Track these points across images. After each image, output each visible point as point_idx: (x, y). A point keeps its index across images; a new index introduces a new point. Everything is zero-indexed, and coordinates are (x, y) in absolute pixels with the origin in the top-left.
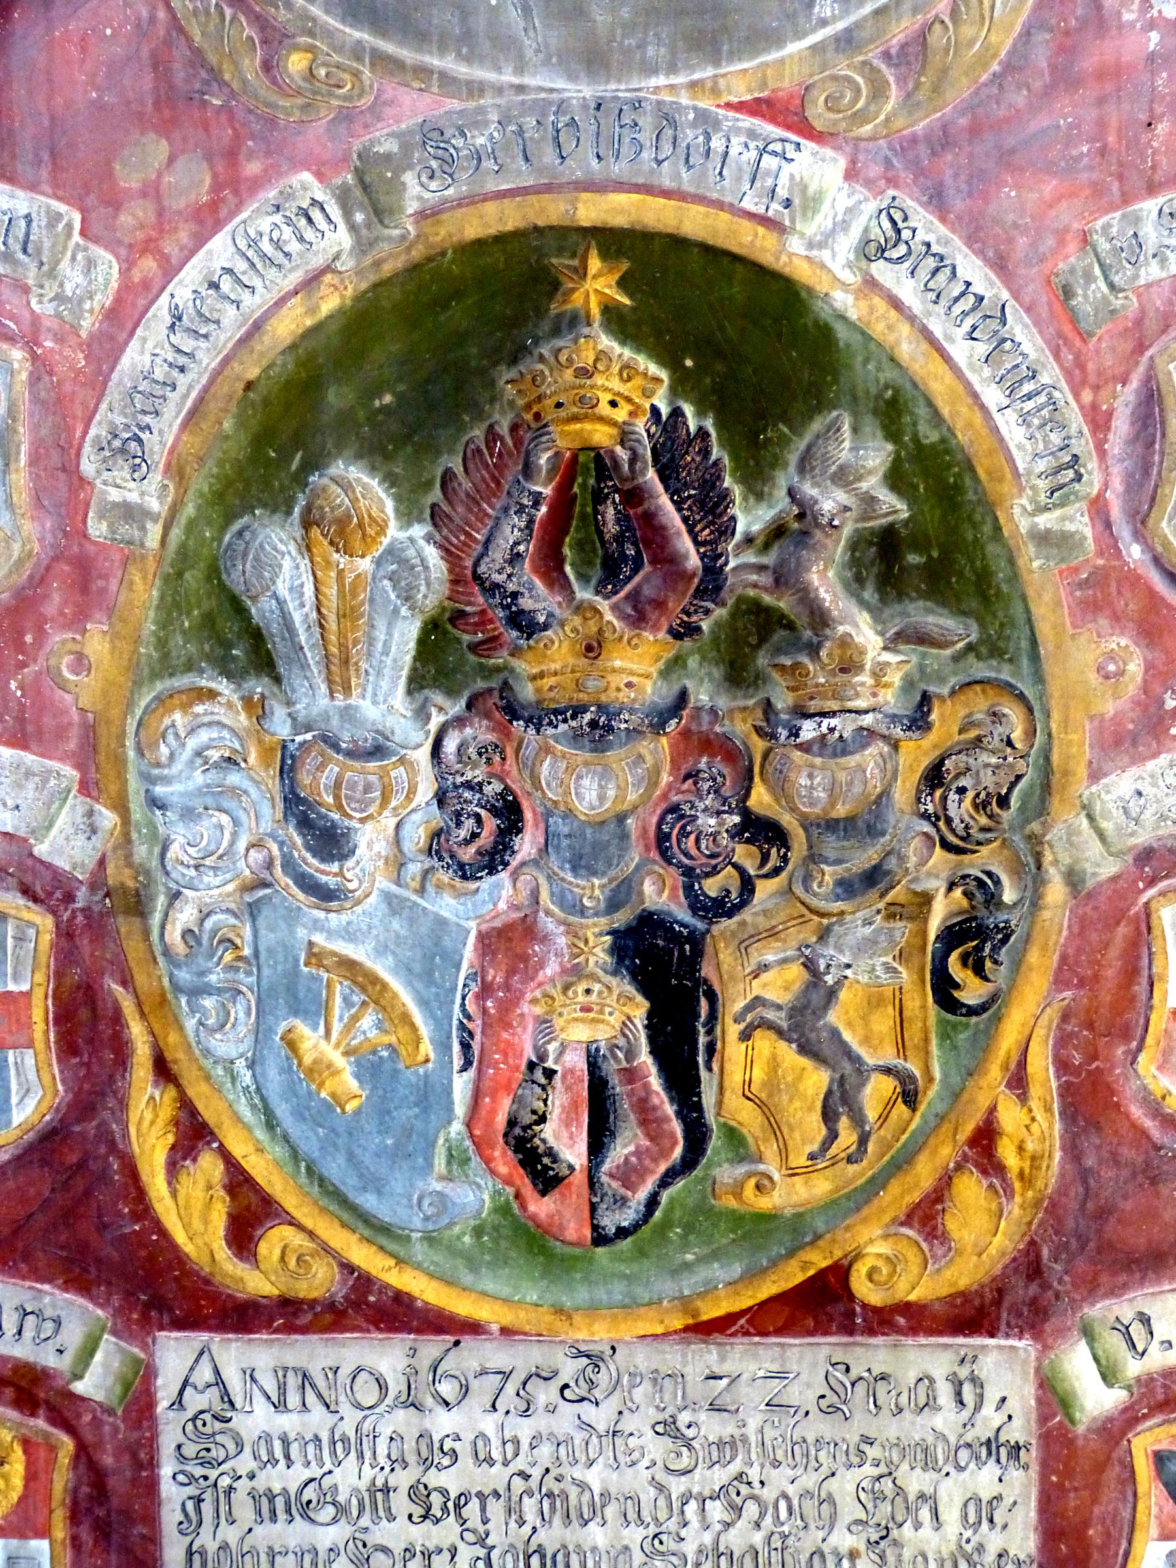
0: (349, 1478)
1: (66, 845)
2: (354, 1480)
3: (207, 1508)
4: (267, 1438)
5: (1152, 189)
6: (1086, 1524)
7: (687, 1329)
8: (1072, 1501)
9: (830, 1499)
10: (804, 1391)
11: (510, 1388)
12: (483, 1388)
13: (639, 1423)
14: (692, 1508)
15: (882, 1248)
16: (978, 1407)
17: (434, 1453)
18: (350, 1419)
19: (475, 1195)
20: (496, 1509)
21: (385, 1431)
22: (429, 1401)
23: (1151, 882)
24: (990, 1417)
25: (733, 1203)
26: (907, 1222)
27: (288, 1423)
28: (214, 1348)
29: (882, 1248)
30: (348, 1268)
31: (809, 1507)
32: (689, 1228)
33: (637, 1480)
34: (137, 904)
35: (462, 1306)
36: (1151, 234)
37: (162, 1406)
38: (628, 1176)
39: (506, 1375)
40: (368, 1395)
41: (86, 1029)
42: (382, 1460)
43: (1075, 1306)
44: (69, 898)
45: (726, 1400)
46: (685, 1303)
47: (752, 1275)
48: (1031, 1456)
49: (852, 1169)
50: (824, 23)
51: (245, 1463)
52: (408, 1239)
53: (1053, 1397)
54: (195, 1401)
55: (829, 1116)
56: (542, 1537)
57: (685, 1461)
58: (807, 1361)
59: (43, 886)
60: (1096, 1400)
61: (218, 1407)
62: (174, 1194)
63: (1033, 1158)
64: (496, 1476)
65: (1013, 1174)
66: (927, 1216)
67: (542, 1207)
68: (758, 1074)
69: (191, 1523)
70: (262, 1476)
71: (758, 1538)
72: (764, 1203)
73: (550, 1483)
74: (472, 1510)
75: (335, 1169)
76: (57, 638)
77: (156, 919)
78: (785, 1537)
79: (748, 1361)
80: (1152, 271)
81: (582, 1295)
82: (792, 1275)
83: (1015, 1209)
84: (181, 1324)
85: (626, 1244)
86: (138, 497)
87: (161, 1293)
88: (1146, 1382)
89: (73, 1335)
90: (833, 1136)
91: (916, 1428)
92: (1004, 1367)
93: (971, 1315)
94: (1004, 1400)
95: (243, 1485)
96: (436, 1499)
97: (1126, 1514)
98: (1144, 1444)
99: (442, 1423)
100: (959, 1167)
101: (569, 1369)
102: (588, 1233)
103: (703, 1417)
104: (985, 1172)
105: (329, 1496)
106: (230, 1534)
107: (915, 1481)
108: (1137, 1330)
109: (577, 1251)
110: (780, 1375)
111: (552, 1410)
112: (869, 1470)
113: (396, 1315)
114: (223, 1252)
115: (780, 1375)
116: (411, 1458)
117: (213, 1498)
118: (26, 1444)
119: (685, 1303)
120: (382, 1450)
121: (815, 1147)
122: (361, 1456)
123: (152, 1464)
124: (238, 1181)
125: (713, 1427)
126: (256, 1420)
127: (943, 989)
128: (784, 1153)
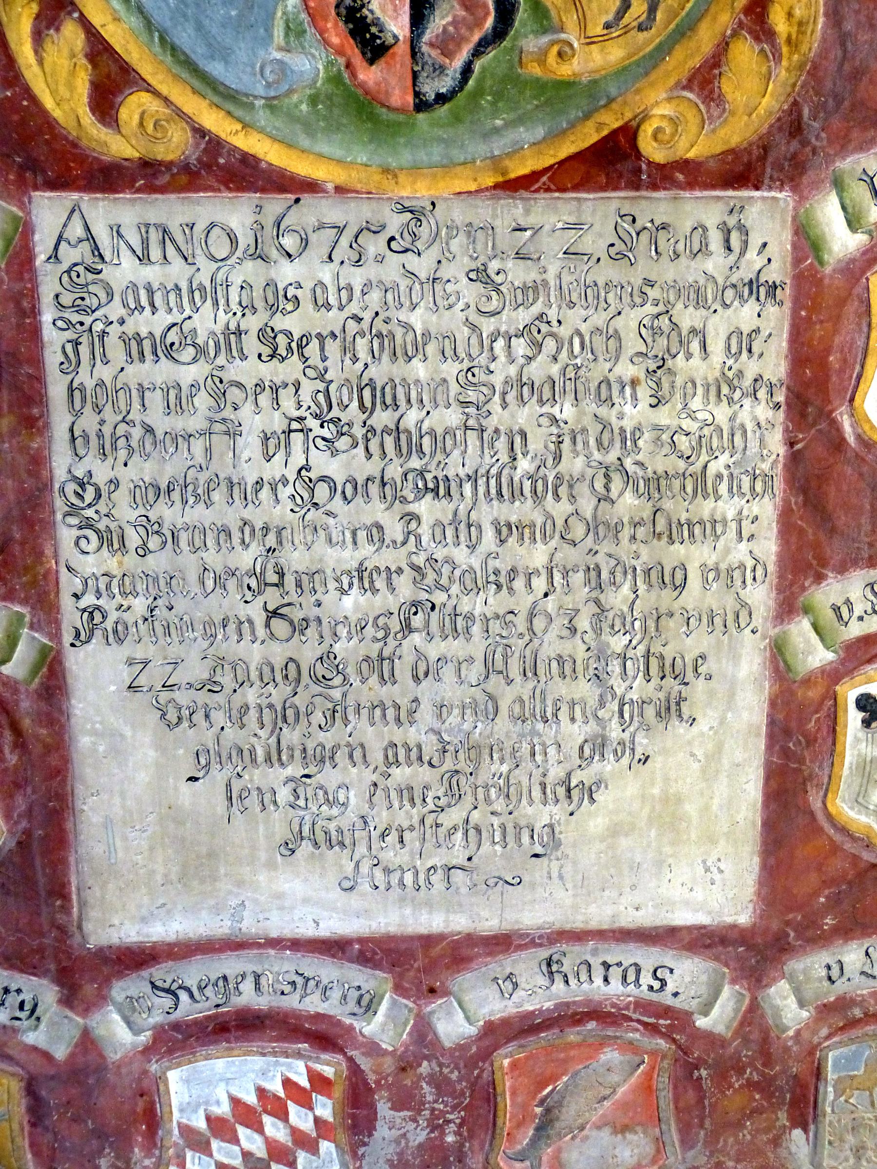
0: (206, 322)
2: (211, 325)
3: (84, 350)
6: (828, 351)
7: (496, 186)
8: (818, 331)
9: (617, 335)
10: (595, 242)
11: (344, 241)
12: (321, 241)
13: (455, 272)
14: (500, 344)
15: (666, 110)
16: (743, 253)
17: (279, 299)
18: (207, 268)
19: (310, 64)
20: (333, 348)
21: (237, 280)
22: (274, 254)
24: (753, 260)
25: (536, 70)
26: (688, 86)
27: (151, 274)
28: (84, 207)
29: (666, 110)
30: (200, 132)
31: (599, 342)
32: (498, 96)
33: (453, 321)
38: (447, 44)
42: (235, 307)
43: (829, 160)
45: (530, 249)
46: (496, 163)
47: (555, 136)
48: (785, 294)
49: (642, 36)
51: (115, 311)
52: (251, 106)
53: (806, 241)
54: (69, 255)
56: (373, 372)
57: (494, 304)
58: (598, 213)
61: (89, 260)
62: (41, 62)
63: (800, 24)
64: (333, 319)
65: (781, 40)
66: (705, 81)
67: (370, 75)
69: (71, 363)
70: (130, 321)
72: (565, 70)
73: (379, 325)
75: (185, 37)
78: (578, 368)
79: (550, 213)
81: (406, 157)
82: (588, 136)
83: (782, 73)
84: (53, 185)
85: (443, 110)
91: (690, 271)
92: (766, 214)
93: (740, 171)
94: (765, 245)
95: (114, 330)
96: (282, 340)
97: (860, 343)
99: (286, 273)
100: (735, 34)
101: (395, 222)
102: (410, 99)
103: (510, 264)
104: (757, 39)
105: (189, 339)
106: (105, 373)
107: (688, 317)
109: (402, 118)
110: (576, 226)
111: (380, 260)
112: (649, 309)
113: (243, 175)
114: (88, 118)
115: (576, 226)
116: (259, 304)
117: (88, 341)
119: (496, 163)
120: (234, 297)
121: (610, 17)
122: (216, 303)
123: (35, 312)
124: (99, 49)
125: (518, 274)
126: (124, 271)
128: (583, 24)
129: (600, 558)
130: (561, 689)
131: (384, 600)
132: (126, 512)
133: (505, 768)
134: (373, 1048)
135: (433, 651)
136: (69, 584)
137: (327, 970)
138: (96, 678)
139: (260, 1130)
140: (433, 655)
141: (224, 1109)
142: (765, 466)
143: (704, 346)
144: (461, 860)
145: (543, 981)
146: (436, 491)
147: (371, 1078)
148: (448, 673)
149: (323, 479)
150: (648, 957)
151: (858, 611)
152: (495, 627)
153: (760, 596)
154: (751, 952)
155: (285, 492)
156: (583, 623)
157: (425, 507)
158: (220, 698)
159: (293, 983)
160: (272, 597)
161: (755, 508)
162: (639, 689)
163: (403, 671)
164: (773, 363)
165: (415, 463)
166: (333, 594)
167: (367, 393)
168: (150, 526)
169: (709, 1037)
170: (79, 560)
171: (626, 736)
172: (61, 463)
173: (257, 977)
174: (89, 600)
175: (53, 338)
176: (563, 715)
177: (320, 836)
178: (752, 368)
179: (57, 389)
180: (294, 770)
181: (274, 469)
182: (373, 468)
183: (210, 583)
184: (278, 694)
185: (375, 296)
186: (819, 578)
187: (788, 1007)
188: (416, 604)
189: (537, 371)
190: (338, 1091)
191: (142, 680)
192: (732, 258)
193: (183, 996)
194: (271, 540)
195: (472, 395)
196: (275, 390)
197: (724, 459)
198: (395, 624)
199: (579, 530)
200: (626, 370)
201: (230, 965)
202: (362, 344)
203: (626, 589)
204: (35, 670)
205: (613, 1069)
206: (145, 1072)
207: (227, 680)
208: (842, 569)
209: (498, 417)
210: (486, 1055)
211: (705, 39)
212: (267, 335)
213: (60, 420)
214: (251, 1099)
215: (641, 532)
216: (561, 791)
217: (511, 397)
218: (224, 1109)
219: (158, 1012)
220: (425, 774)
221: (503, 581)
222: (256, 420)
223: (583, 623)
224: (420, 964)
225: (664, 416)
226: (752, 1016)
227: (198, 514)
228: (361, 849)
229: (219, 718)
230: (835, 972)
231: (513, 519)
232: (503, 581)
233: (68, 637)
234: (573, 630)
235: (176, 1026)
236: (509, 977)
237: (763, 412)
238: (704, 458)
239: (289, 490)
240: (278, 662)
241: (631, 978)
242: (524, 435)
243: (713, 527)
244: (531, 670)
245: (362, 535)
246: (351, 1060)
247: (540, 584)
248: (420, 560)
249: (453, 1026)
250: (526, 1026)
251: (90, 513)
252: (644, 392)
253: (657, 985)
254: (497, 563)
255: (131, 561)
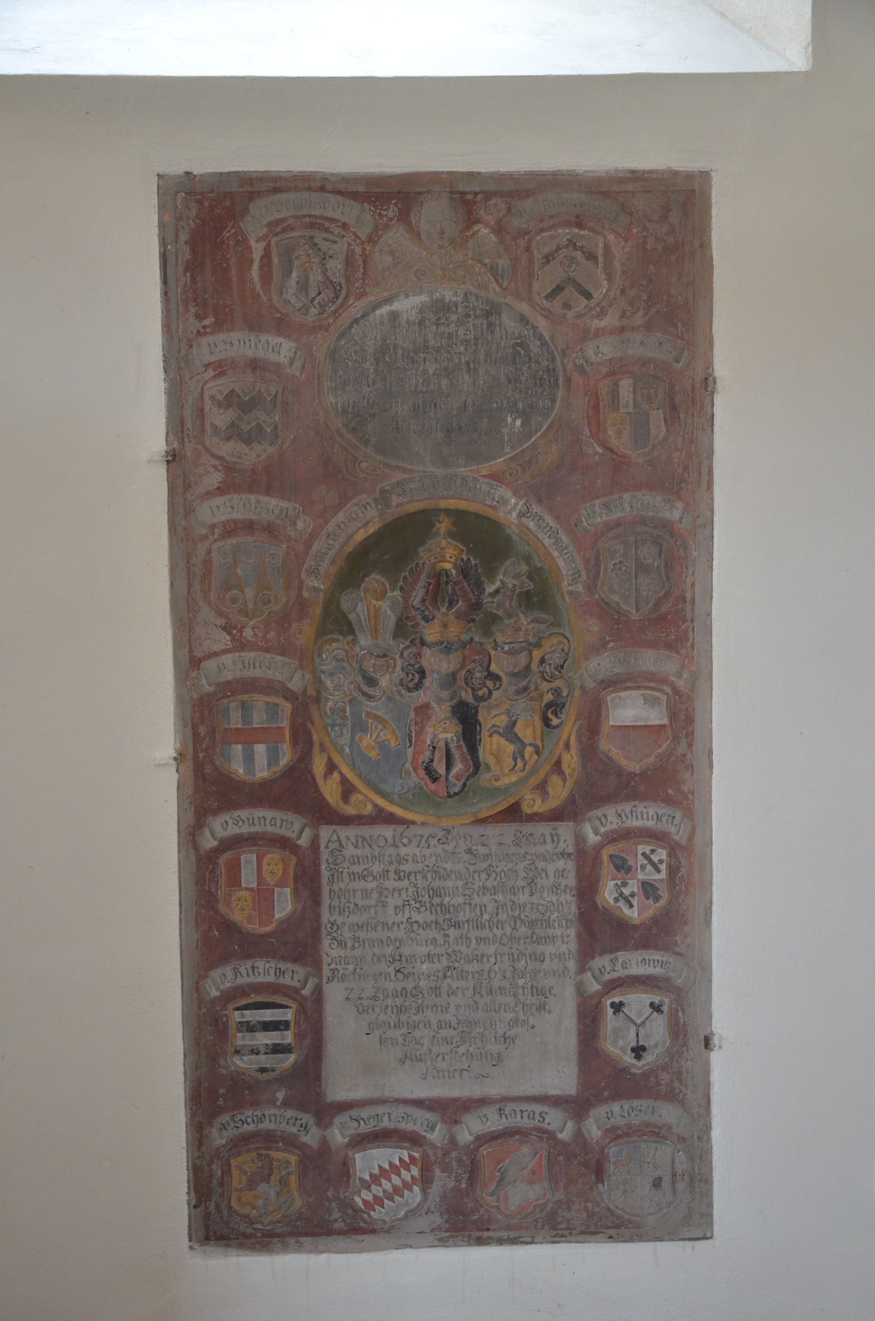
0: (377, 868)
1: (296, 684)
3: (335, 877)
4: (352, 856)
5: (598, 498)
7: (473, 822)
9: (516, 871)
14: (476, 875)
17: (402, 860)
20: (419, 876)
23: (604, 689)
25: (487, 785)
27: (359, 852)
30: (376, 806)
34: (317, 700)
35: (409, 816)
36: (598, 510)
37: (322, 847)
38: (458, 777)
39: (422, 836)
40: (382, 844)
41: (302, 736)
44: (297, 699)
50: (507, 454)
51: (346, 864)
53: (580, 840)
54: (332, 846)
55: (515, 759)
56: (433, 884)
57: (473, 862)
58: (509, 830)
59: (288, 695)
60: (592, 839)
64: (420, 867)
65: (567, 773)
66: (542, 787)
68: (494, 747)
71: (496, 883)
72: (498, 784)
73: (435, 869)
74: (412, 877)
76: (295, 625)
77: (322, 705)
78: (503, 883)
79: (492, 831)
80: (599, 520)
82: (505, 805)
84: (328, 823)
85: (456, 798)
86: (317, 585)
87: (323, 814)
88: (606, 834)
89: (297, 827)
90: (516, 764)
92: (565, 830)
93: (556, 816)
95: (346, 871)
96: (402, 874)
98: (605, 854)
99: (403, 851)
101: (440, 834)
102: (446, 794)
103: (479, 847)
104: (559, 774)
107: (541, 865)
108: (603, 819)
109: (442, 800)
110: (502, 835)
111: (435, 846)
112: (527, 862)
114: (340, 802)
115: (502, 835)
118: (283, 860)
121: (511, 767)
122: (380, 861)
123: (319, 865)
124: (344, 781)
125: (482, 850)
126: (350, 851)
127: (546, 722)
129: (513, 951)
130: (500, 999)
131: (436, 966)
132: (347, 934)
133: (481, 1030)
134: (433, 1146)
135: (455, 985)
136: (326, 960)
137: (417, 1112)
138: (335, 996)
139: (390, 1180)
140: (455, 987)
141: (376, 1171)
142: (570, 917)
143: (547, 874)
144: (466, 1067)
145: (498, 1117)
146: (455, 926)
147: (433, 1158)
148: (460, 993)
149: (416, 922)
150: (538, 1108)
151: (608, 969)
152: (476, 975)
153: (572, 965)
154: (577, 1107)
155: (402, 927)
156: (508, 974)
157: (452, 932)
158: (378, 1003)
159: (403, 1117)
160: (397, 965)
161: (568, 932)
162: (530, 1000)
163: (444, 991)
164: (571, 880)
165: (448, 916)
166: (419, 964)
167: (431, 892)
168: (356, 939)
169: (563, 1143)
170: (329, 951)
171: (525, 1018)
172: (325, 917)
173: (389, 1114)
174: (333, 966)
175: (325, 874)
176: (502, 1010)
177: (414, 1057)
178: (564, 882)
179: (325, 890)
180: (404, 1031)
181: (399, 918)
182: (433, 918)
183: (375, 960)
184: (399, 1001)
185: (434, 858)
186: (593, 958)
187: (593, 1130)
188: (448, 967)
189: (489, 884)
190: (419, 1164)
191: (350, 996)
192: (555, 844)
193: (362, 1122)
194: (397, 944)
195: (467, 892)
196: (399, 891)
197: (556, 914)
198: (441, 975)
199: (505, 940)
200: (520, 883)
201: (380, 1110)
202: (429, 875)
203: (523, 962)
204: (313, 993)
205: (525, 1156)
206: (347, 1155)
207: (381, 996)
208: (601, 955)
209: (476, 900)
210: (477, 1149)
211: (542, 774)
212: (397, 872)
213: (326, 901)
214: (387, 1167)
215: (528, 941)
216: (502, 1039)
217: (481, 893)
218: (376, 1171)
219: (353, 1129)
220: (452, 1033)
221: (480, 959)
222: (393, 901)
223: (508, 974)
224: (452, 1110)
225: (534, 899)
226: (579, 1134)
227: (373, 935)
228: (429, 1063)
229: (377, 1010)
230: (610, 1115)
231: (482, 936)
232: (480, 959)
233: (325, 980)
234: (504, 977)
235: (358, 1135)
236: (485, 1116)
237: (569, 898)
238: (549, 914)
239: (404, 926)
240: (399, 989)
241: (531, 1116)
242: (485, 906)
243: (553, 939)
244: (490, 992)
245: (429, 942)
246: (425, 1150)
247: (492, 960)
248: (450, 951)
249: (465, 1137)
250: (492, 1137)
251: (335, 934)
252: (527, 891)
253: (541, 1120)
254: (478, 953)
255: (348, 952)
